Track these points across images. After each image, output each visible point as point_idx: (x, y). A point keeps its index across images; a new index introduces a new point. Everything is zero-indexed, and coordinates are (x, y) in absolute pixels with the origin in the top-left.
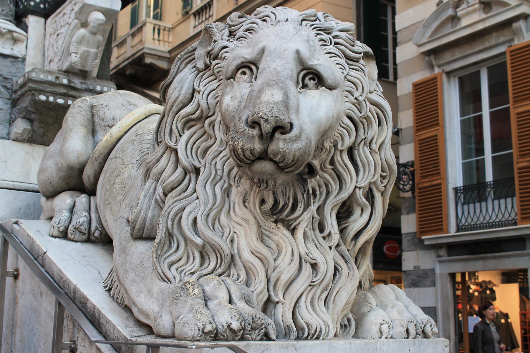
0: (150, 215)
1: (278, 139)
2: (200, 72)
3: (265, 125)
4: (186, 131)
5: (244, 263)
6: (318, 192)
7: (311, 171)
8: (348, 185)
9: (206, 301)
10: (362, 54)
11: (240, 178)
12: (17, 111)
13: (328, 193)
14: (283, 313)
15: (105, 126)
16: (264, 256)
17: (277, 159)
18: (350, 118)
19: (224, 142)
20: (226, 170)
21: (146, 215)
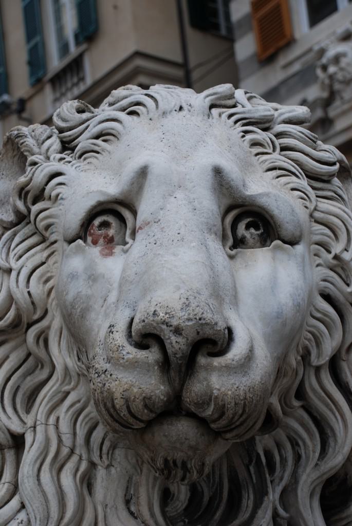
2: (6, 229)
3: (174, 338)
6: (277, 458)
10: (338, 165)
11: (114, 447)
13: (298, 458)
17: (209, 412)
18: (327, 297)
19: (73, 374)
20: (81, 432)
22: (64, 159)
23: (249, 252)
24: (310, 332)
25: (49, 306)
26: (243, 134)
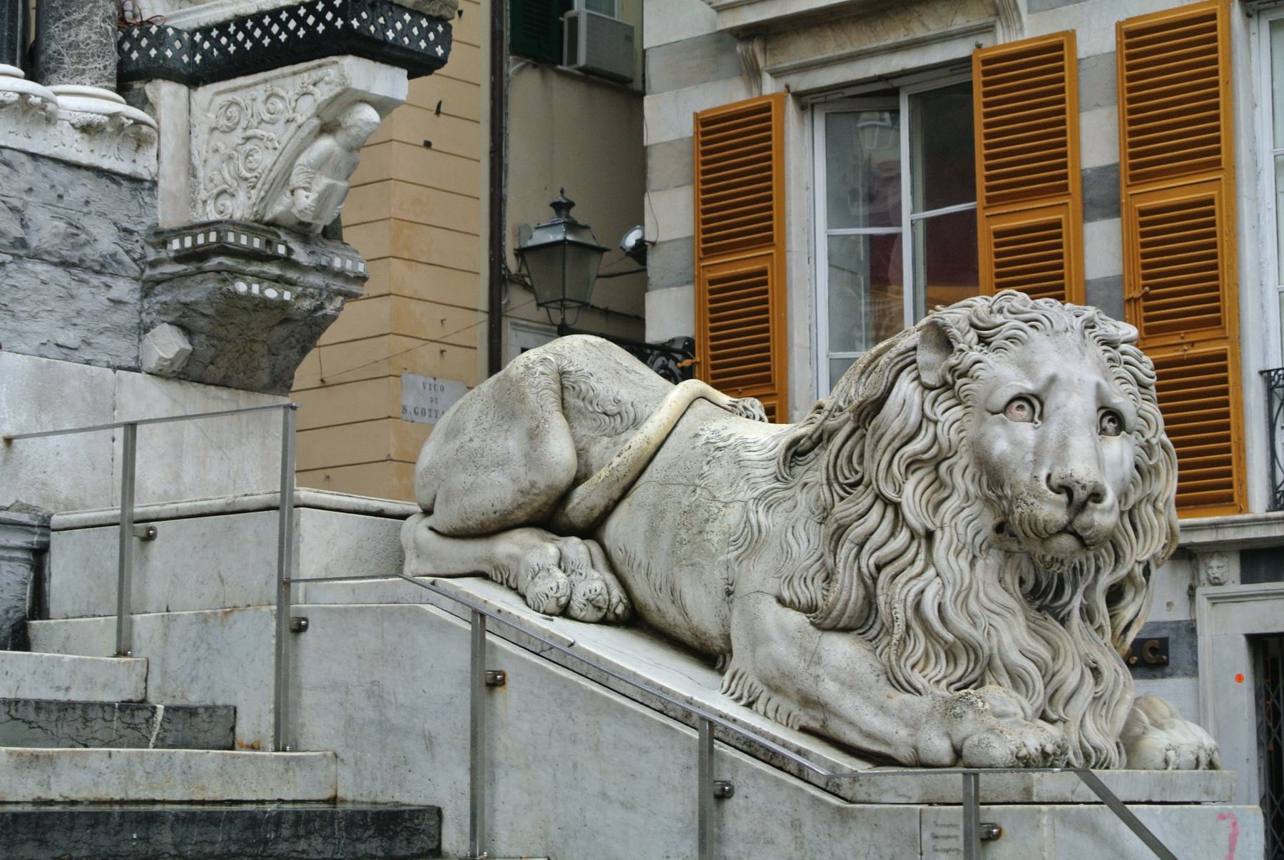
1: (1094, 509)
11: (990, 547)
12: (157, 307)
13: (1098, 569)
15: (594, 412)
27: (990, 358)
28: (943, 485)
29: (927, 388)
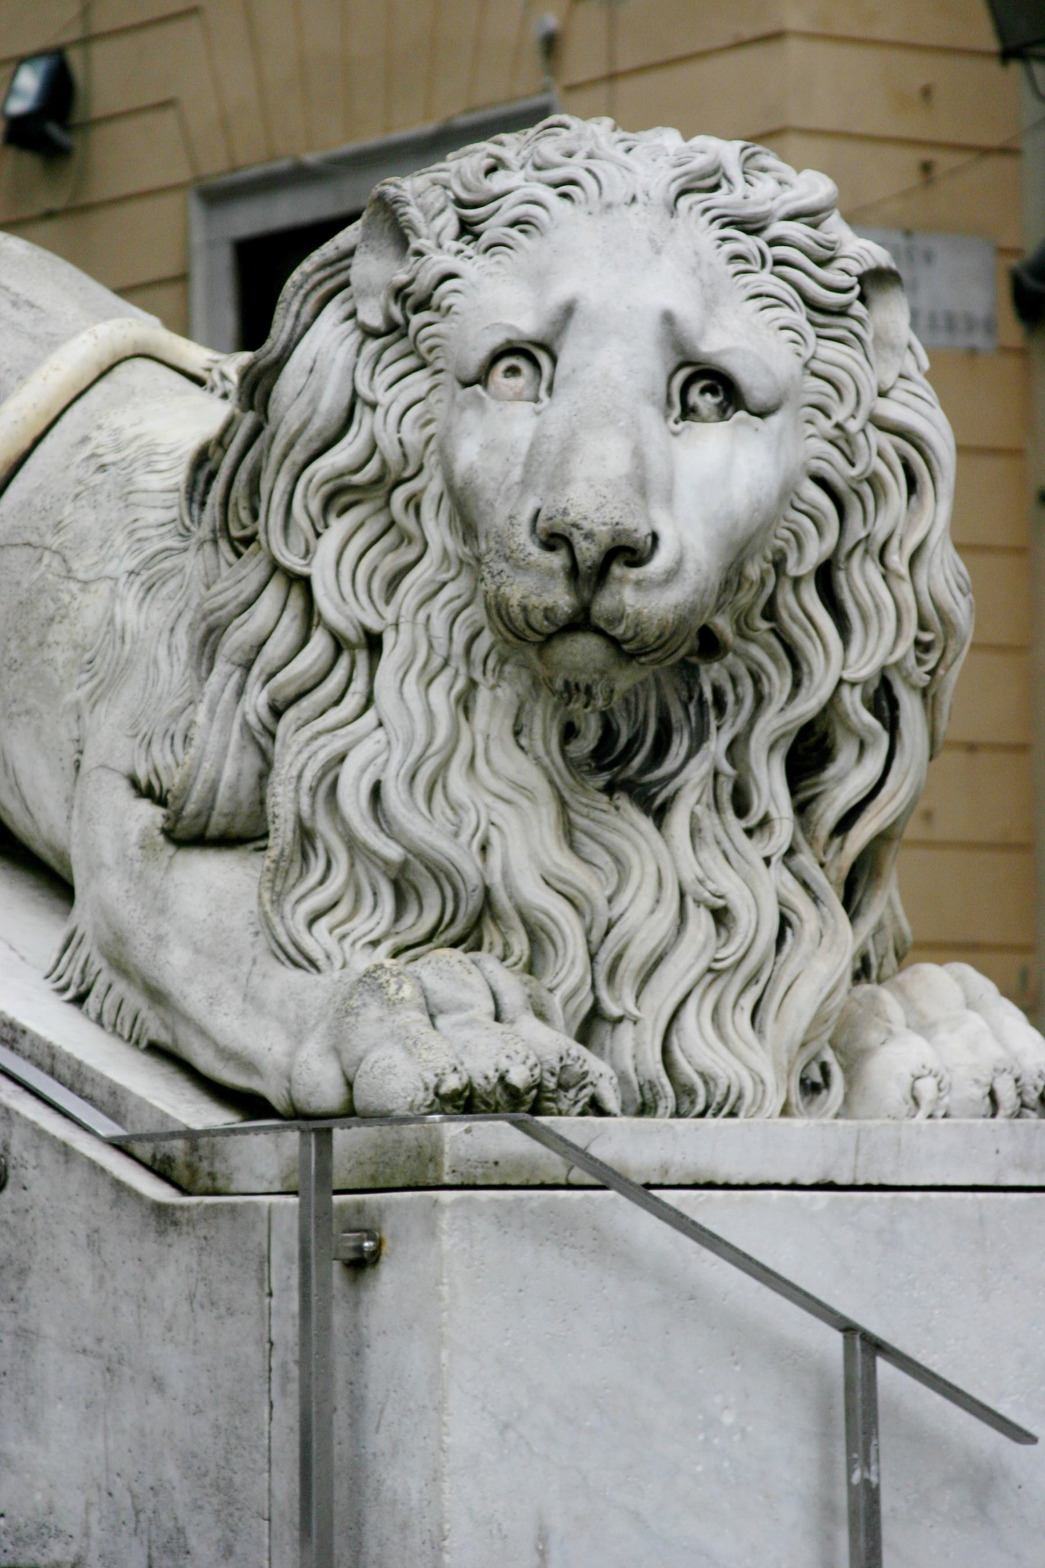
0: (228, 773)
1: (621, 581)
4: (332, 520)
5: (525, 911)
6: (730, 698)
7: (710, 644)
8: (817, 678)
9: (432, 1017)
13: (760, 700)
14: (636, 1048)
16: (581, 892)
17: (619, 631)
18: (821, 482)
20: (460, 637)
21: (219, 772)
22: (461, 251)
23: (697, 427)
24: (789, 529)
25: (425, 461)
26: (719, 242)
27: (473, 266)
28: (405, 539)
29: (370, 333)
